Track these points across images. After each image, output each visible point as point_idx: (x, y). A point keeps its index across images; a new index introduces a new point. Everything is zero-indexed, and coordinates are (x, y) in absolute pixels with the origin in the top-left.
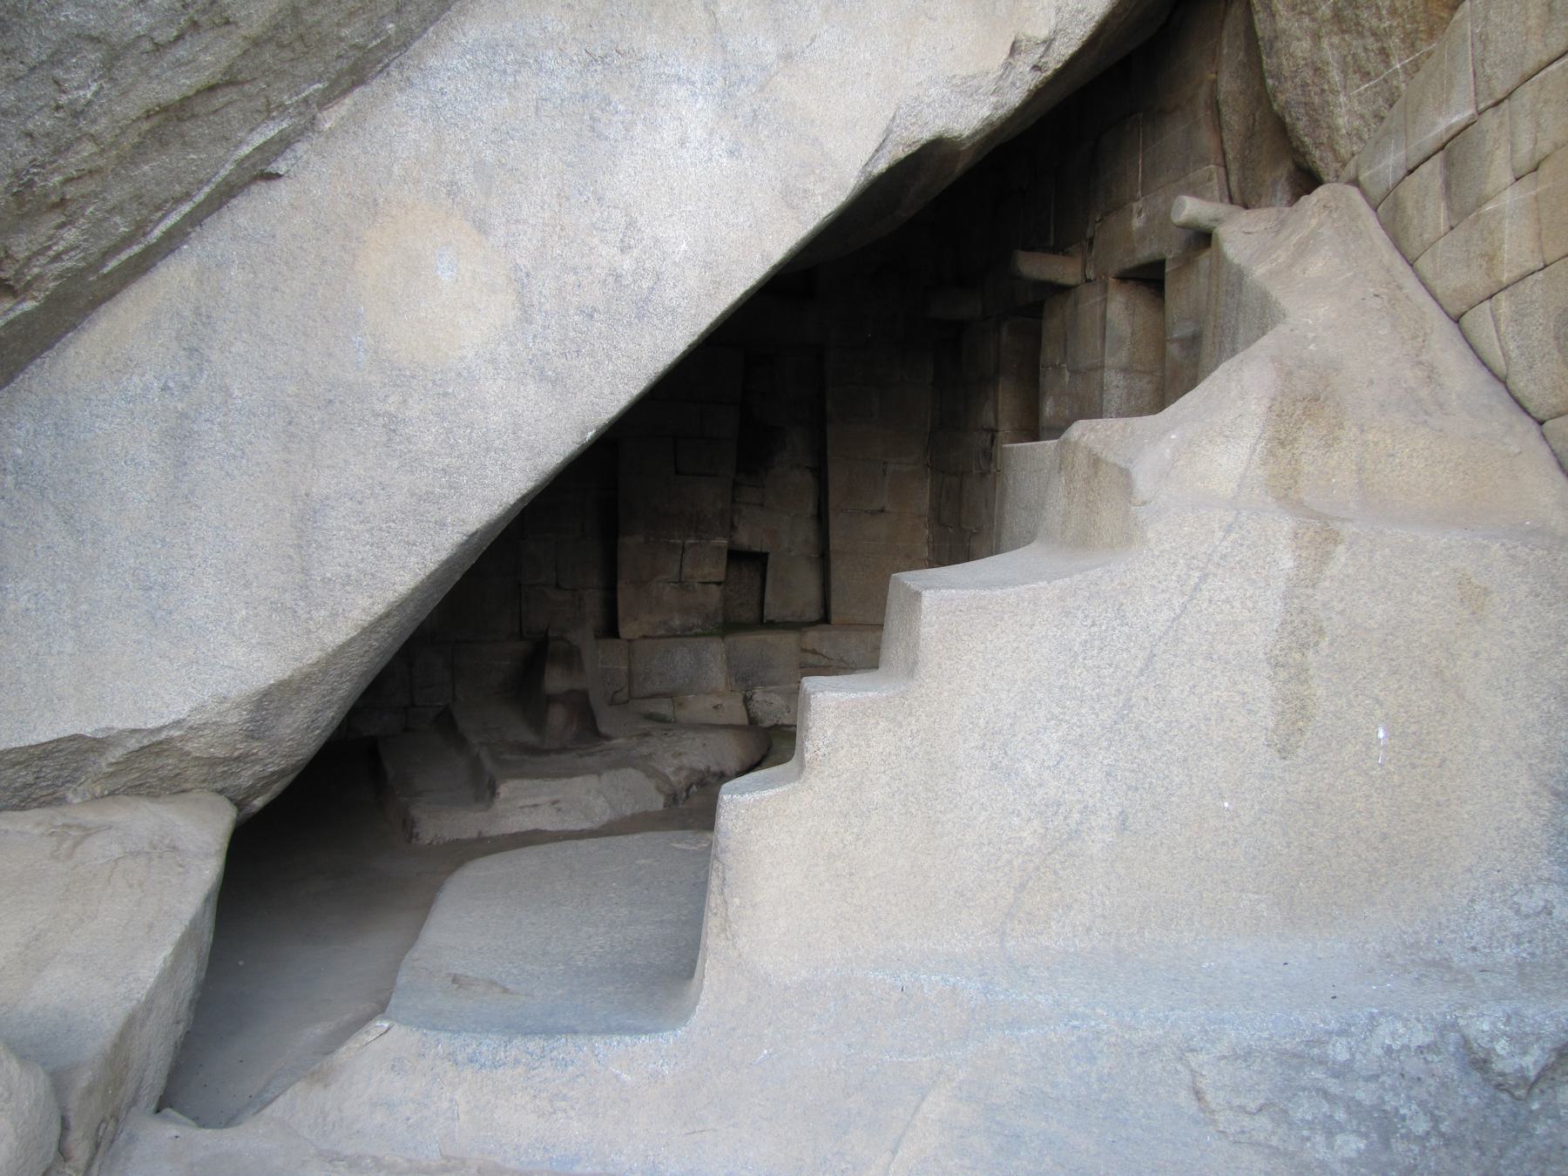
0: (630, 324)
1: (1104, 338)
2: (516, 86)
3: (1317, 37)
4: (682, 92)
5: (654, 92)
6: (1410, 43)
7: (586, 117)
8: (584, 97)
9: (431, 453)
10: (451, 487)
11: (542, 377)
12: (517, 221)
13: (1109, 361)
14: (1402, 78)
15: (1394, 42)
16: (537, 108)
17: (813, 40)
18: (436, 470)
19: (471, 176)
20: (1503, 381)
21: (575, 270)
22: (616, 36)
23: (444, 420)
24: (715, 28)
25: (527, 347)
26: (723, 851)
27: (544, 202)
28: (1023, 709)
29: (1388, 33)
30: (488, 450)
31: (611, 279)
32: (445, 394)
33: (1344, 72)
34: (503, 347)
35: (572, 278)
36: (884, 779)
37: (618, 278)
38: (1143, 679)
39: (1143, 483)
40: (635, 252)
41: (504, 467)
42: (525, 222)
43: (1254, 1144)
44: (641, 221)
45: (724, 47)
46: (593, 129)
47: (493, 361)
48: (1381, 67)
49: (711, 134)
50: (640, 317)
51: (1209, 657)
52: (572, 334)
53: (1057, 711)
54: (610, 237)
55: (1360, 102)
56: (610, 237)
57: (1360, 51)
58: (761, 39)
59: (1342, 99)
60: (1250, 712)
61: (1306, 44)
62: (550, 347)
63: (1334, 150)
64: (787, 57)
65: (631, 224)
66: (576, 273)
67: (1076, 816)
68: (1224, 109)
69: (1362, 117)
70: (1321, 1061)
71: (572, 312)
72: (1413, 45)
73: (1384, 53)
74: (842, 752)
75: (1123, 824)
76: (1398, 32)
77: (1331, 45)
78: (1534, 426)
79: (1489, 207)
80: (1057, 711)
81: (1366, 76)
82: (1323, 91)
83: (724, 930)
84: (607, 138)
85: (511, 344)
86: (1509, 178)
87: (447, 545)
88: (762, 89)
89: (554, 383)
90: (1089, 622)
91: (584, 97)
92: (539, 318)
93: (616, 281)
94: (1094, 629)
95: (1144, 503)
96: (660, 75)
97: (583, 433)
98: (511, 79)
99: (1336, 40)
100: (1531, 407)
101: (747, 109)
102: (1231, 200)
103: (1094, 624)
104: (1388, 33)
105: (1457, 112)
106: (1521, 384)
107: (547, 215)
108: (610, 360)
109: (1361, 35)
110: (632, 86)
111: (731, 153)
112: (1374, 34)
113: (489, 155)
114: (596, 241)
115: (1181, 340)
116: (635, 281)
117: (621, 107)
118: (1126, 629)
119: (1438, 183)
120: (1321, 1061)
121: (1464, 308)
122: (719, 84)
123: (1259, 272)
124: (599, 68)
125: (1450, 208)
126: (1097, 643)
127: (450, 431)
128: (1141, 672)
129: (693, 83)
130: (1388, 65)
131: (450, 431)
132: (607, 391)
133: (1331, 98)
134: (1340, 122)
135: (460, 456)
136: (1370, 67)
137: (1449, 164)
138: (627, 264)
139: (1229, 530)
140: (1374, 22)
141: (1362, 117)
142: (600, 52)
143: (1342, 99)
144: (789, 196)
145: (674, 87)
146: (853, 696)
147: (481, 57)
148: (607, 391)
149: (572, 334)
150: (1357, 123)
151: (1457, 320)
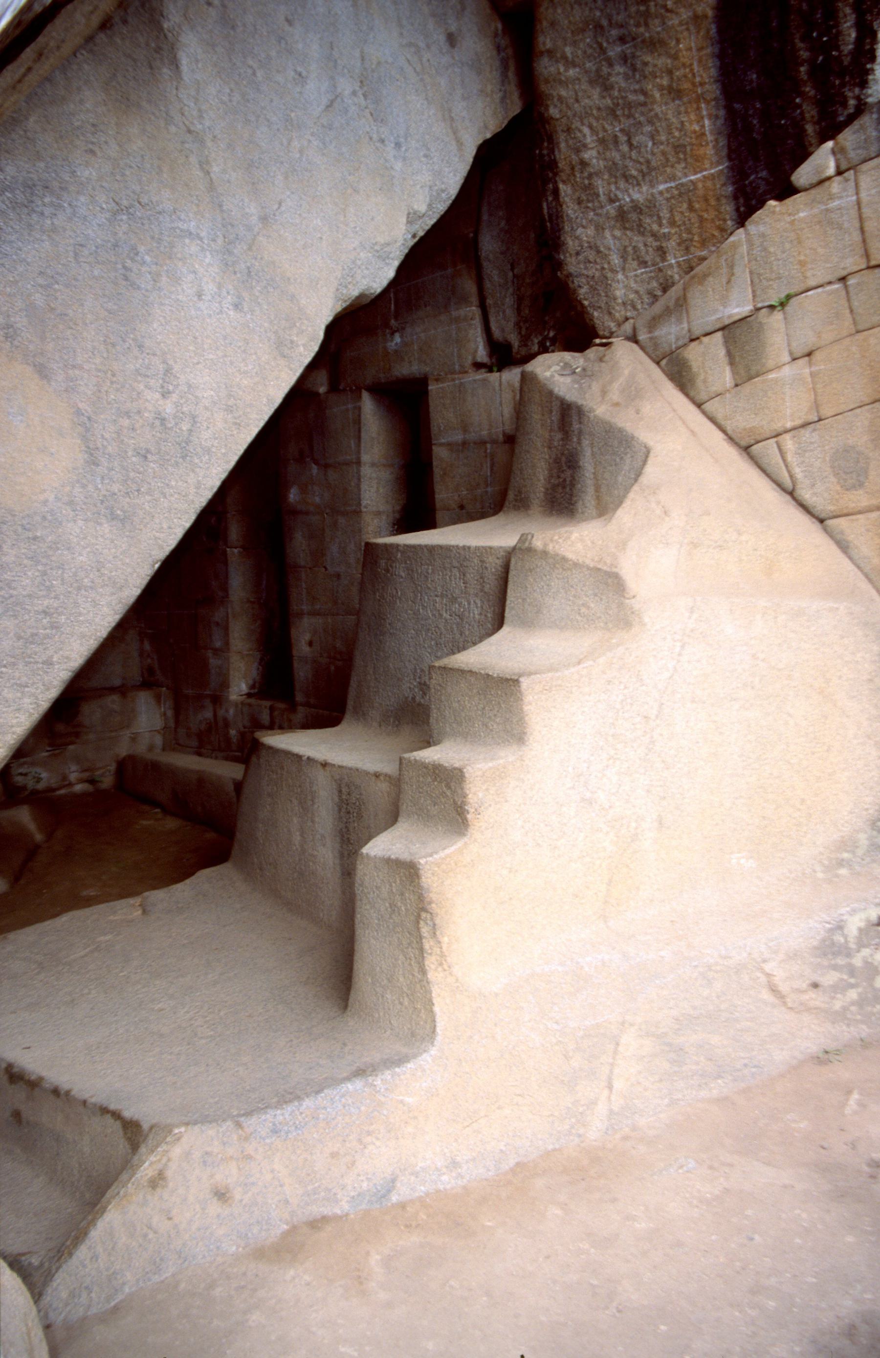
0: (177, 463)
1: (359, 438)
2: (54, 229)
3: (599, 228)
4: (194, 249)
5: (172, 246)
6: (685, 246)
7: (120, 266)
8: (116, 246)
9: (30, 596)
10: (52, 627)
11: (113, 517)
12: (74, 367)
13: (365, 458)
14: (676, 270)
15: (672, 244)
16: (76, 255)
17: (280, 204)
18: (38, 612)
19: (25, 320)
20: (791, 493)
21: (127, 414)
22: (138, 188)
23: (38, 562)
24: (211, 187)
25: (97, 489)
26: (430, 903)
27: (94, 348)
28: (592, 755)
29: (667, 237)
30: (79, 589)
31: (157, 423)
32: (35, 538)
34: (78, 490)
35: (126, 422)
36: (520, 823)
37: (163, 420)
38: (658, 721)
40: (174, 397)
41: (95, 603)
42: (81, 368)
43: (809, 1010)
44: (177, 368)
45: (220, 206)
46: (126, 279)
47: (71, 503)
48: (658, 259)
49: (219, 288)
50: (184, 458)
51: (693, 701)
52: (132, 474)
53: (612, 752)
54: (152, 382)
55: (636, 282)
56: (152, 382)
57: (641, 246)
58: (246, 200)
59: (620, 276)
60: (721, 733)
61: (591, 231)
62: (115, 488)
63: (610, 313)
64: (264, 219)
65: (168, 371)
66: (129, 417)
67: (634, 825)
68: (485, 264)
69: (637, 292)
71: (130, 453)
72: (687, 249)
73: (662, 252)
74: (491, 809)
76: (675, 237)
77: (614, 237)
78: (815, 526)
79: (771, 376)
80: (612, 752)
81: (643, 263)
82: (603, 268)
83: (441, 964)
84: (139, 288)
85: (84, 486)
86: (787, 358)
87: (56, 683)
88: (250, 249)
89: (122, 521)
90: (622, 687)
91: (116, 246)
92: (104, 461)
93: (162, 424)
94: (626, 691)
95: (634, 597)
96: (174, 229)
97: (153, 566)
98: (49, 222)
99: (618, 233)
100: (814, 511)
101: (243, 266)
103: (626, 688)
104: (667, 237)
105: (738, 306)
106: (806, 495)
107: (98, 361)
108: (165, 497)
109: (643, 234)
110: (153, 238)
111: (237, 306)
112: (654, 235)
113: (39, 299)
114: (142, 387)
115: (450, 445)
116: (177, 424)
117: (148, 259)
118: (644, 688)
119: (722, 352)
121: (753, 442)
122: (220, 241)
124: (125, 217)
125: (734, 373)
126: (629, 701)
127: (44, 573)
128: (657, 717)
129: (201, 239)
130: (664, 259)
131: (44, 573)
132: (165, 526)
133: (609, 275)
134: (618, 293)
135: (56, 597)
136: (648, 258)
137: (728, 343)
138: (168, 408)
139: (692, 611)
140: (655, 227)
141: (637, 292)
142: (125, 203)
143: (620, 276)
144: (281, 347)
145: (187, 241)
146: (490, 765)
147: (20, 198)
148: (165, 526)
149: (132, 474)
150: (632, 296)
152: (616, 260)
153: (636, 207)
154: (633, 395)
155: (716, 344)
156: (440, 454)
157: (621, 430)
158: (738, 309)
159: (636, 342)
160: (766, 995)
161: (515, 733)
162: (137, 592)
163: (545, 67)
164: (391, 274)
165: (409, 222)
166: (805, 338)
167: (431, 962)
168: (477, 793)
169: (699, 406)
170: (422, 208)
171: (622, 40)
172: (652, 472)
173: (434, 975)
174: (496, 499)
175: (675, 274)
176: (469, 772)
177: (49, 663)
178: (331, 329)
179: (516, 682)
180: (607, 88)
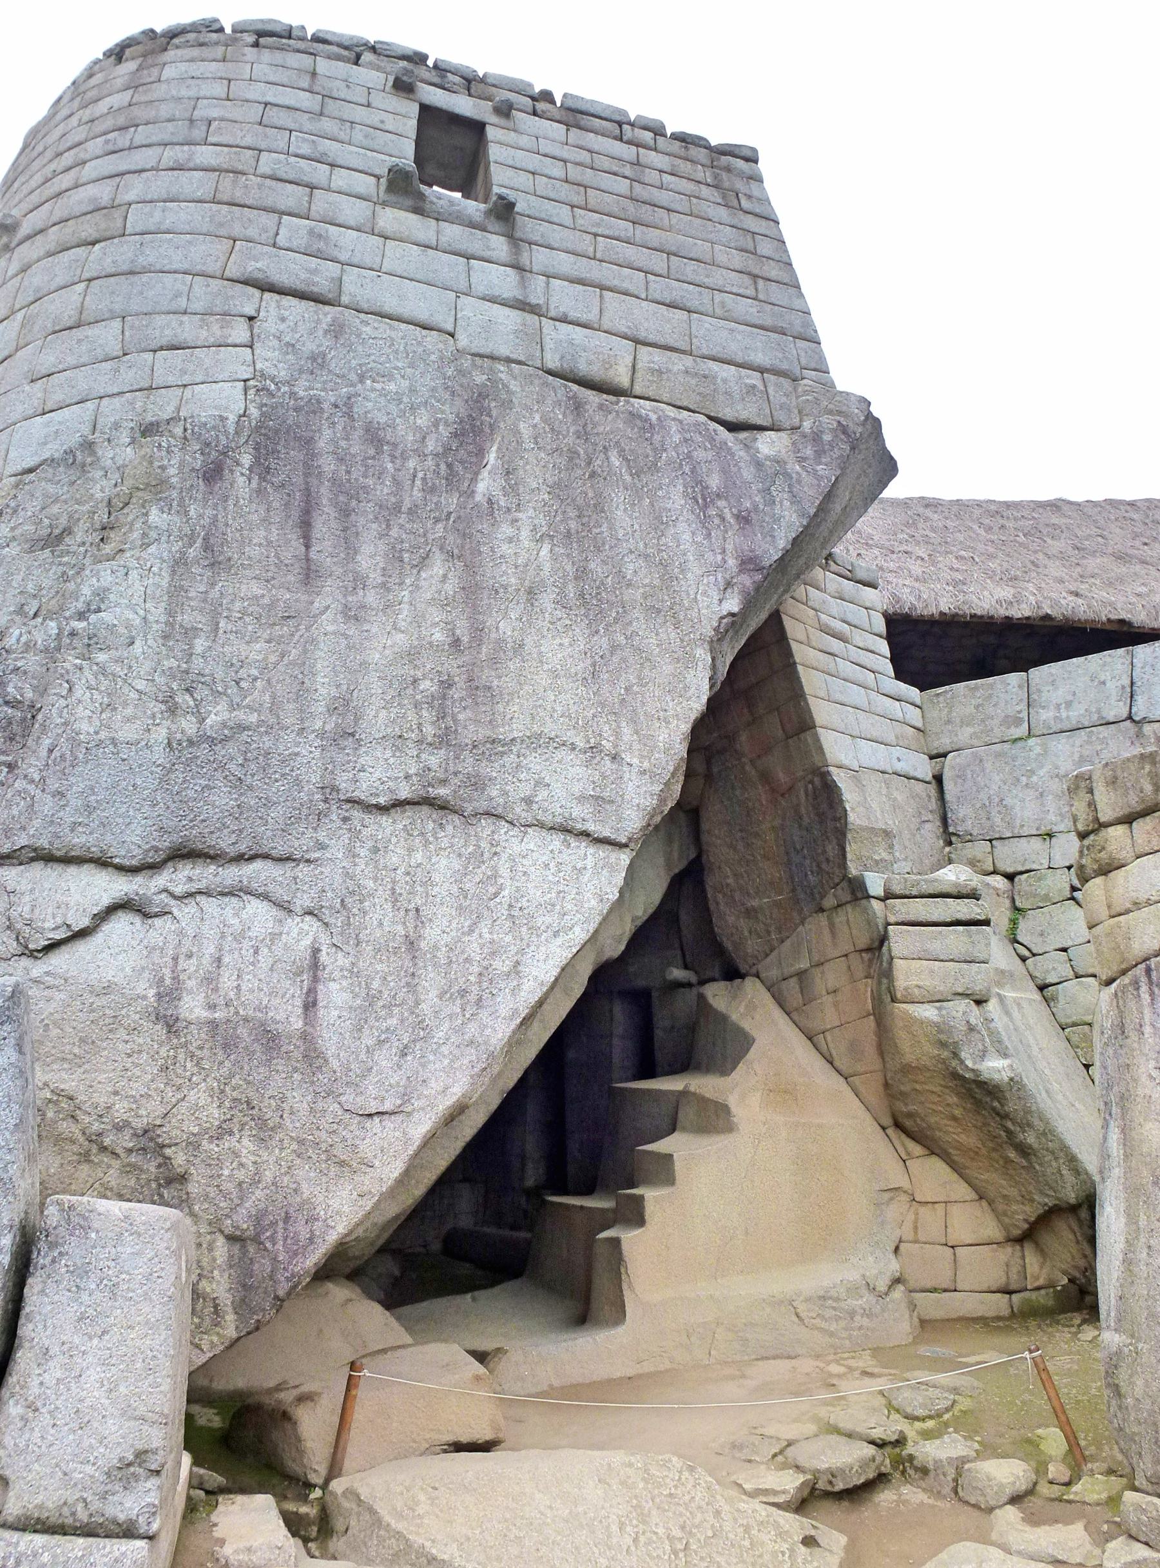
3: (738, 917)
6: (779, 930)
15: (772, 928)
33: (750, 932)
39: (734, 1109)
70: (830, 1298)
73: (769, 932)
75: (747, 1233)
102: (686, 967)
106: (837, 1063)
120: (830, 1298)
123: (734, 1017)
137: (801, 982)
151: (810, 1039)
152: (746, 933)
153: (754, 910)
154: (752, 1007)
155: (793, 982)
156: (659, 1034)
157: (743, 1029)
158: (804, 965)
159: (758, 977)
160: (796, 1320)
161: (670, 1180)
162: (495, 1107)
163: (705, 838)
164: (623, 948)
165: (633, 921)
166: (832, 983)
167: (625, 1286)
168: (650, 1208)
169: (788, 1014)
170: (640, 913)
171: (741, 831)
172: (752, 1050)
173: (627, 1293)
174: (684, 1064)
175: (775, 943)
176: (646, 1196)
177: (457, 1138)
178: (590, 979)
179: (671, 1156)
180: (735, 849)
